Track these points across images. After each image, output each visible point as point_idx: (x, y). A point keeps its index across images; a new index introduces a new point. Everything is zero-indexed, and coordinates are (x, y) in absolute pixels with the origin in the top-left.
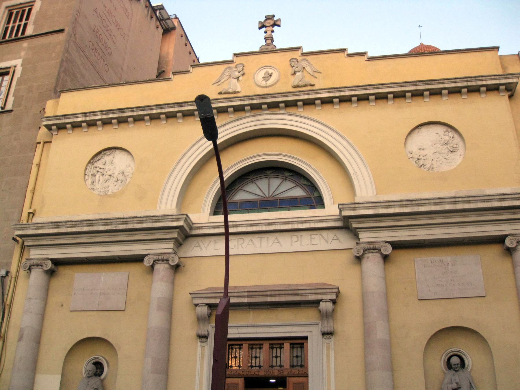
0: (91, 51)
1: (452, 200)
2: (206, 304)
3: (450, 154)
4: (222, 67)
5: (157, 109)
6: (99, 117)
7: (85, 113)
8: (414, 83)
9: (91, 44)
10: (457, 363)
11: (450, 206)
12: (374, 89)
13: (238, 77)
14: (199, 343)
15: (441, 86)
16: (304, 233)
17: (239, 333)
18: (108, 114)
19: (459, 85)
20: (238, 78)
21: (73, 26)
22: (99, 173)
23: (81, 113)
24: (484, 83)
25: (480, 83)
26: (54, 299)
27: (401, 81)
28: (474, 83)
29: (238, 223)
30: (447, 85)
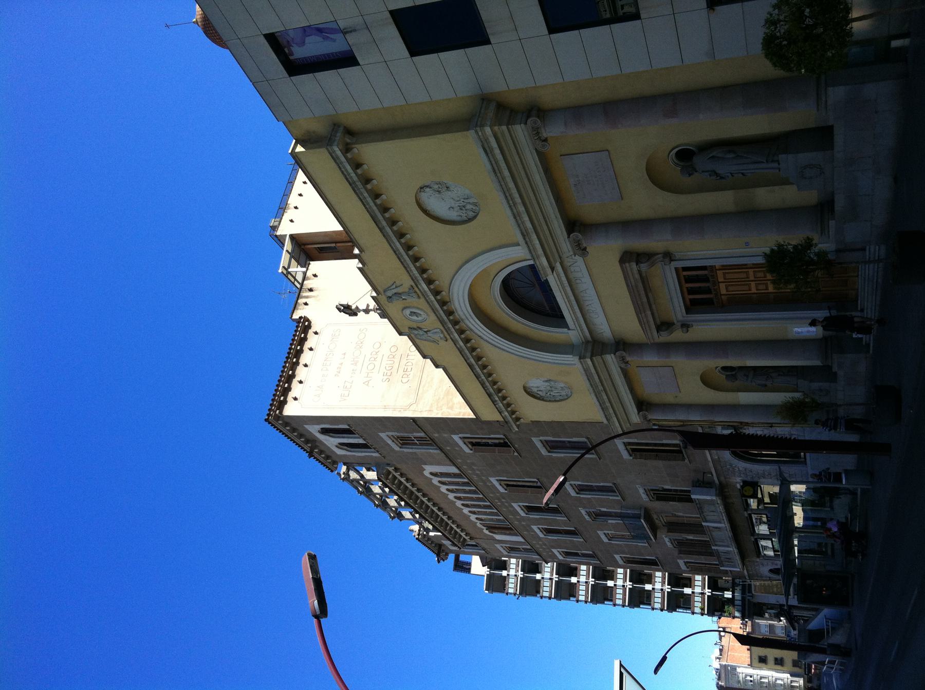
0: (411, 377)
1: (514, 208)
2: (658, 332)
3: (451, 189)
4: (417, 341)
5: (481, 377)
6: (501, 405)
7: (500, 413)
8: (381, 229)
9: (405, 380)
10: (688, 175)
11: (519, 207)
12: (402, 256)
13: (425, 331)
14: (694, 327)
15: (375, 208)
16: (571, 276)
17: (680, 306)
18: (496, 401)
19: (366, 195)
20: (426, 332)
21: (402, 410)
22: (552, 393)
23: (501, 415)
24: (353, 175)
25: (355, 178)
26: (670, 399)
27: (385, 240)
28: (359, 184)
29: (574, 318)
30: (372, 204)
